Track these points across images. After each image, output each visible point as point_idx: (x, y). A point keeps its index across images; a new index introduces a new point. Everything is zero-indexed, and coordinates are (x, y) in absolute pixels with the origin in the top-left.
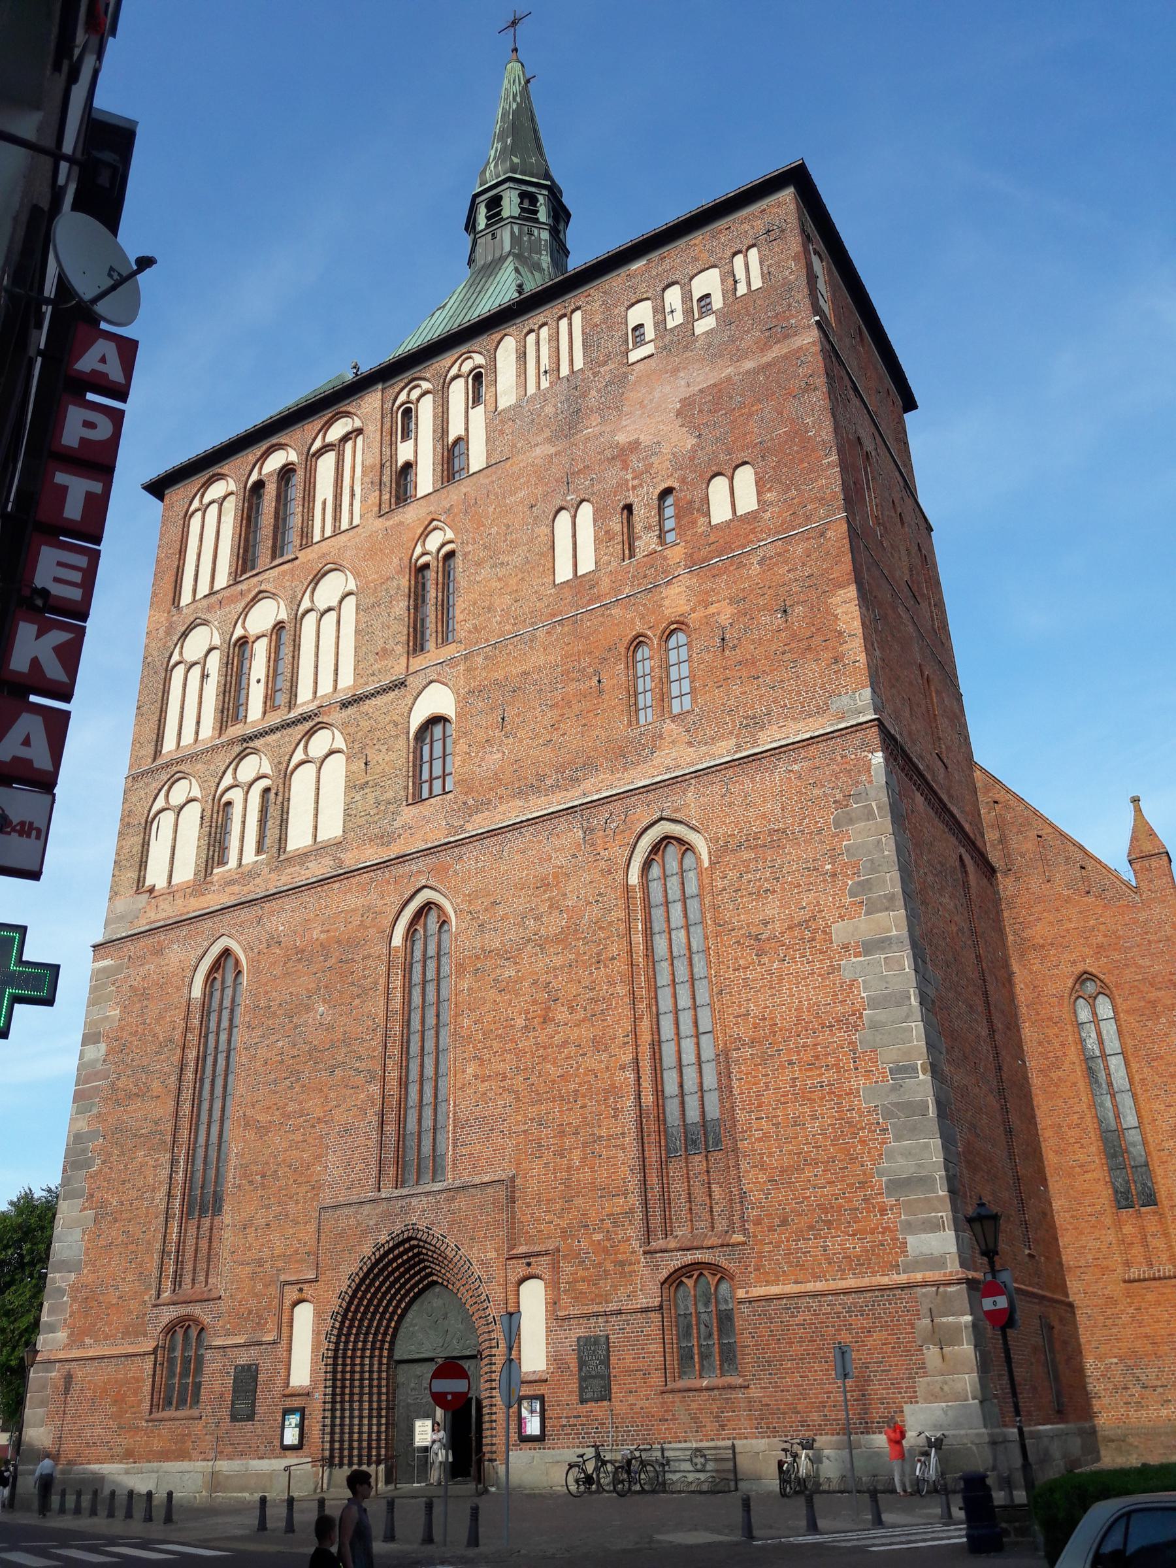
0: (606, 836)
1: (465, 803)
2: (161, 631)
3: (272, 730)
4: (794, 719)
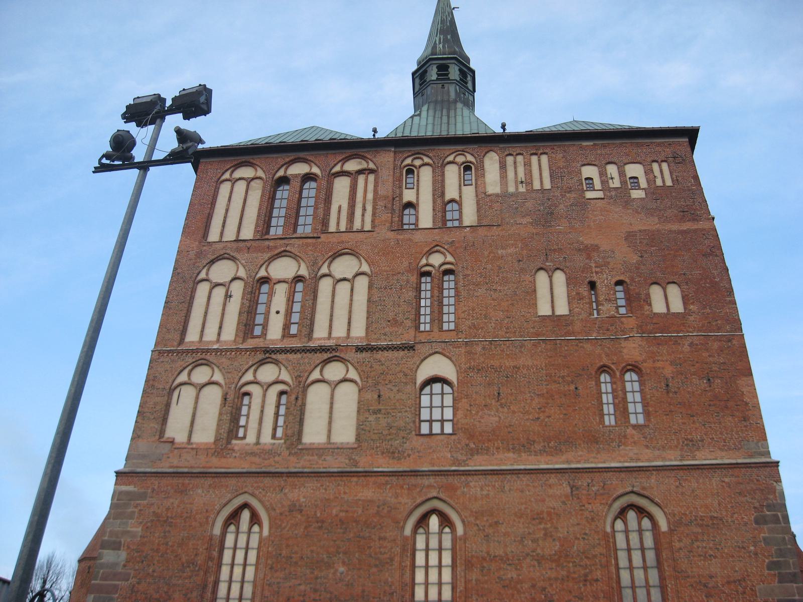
0: (589, 495)
1: (467, 445)
2: (192, 254)
4: (720, 449)
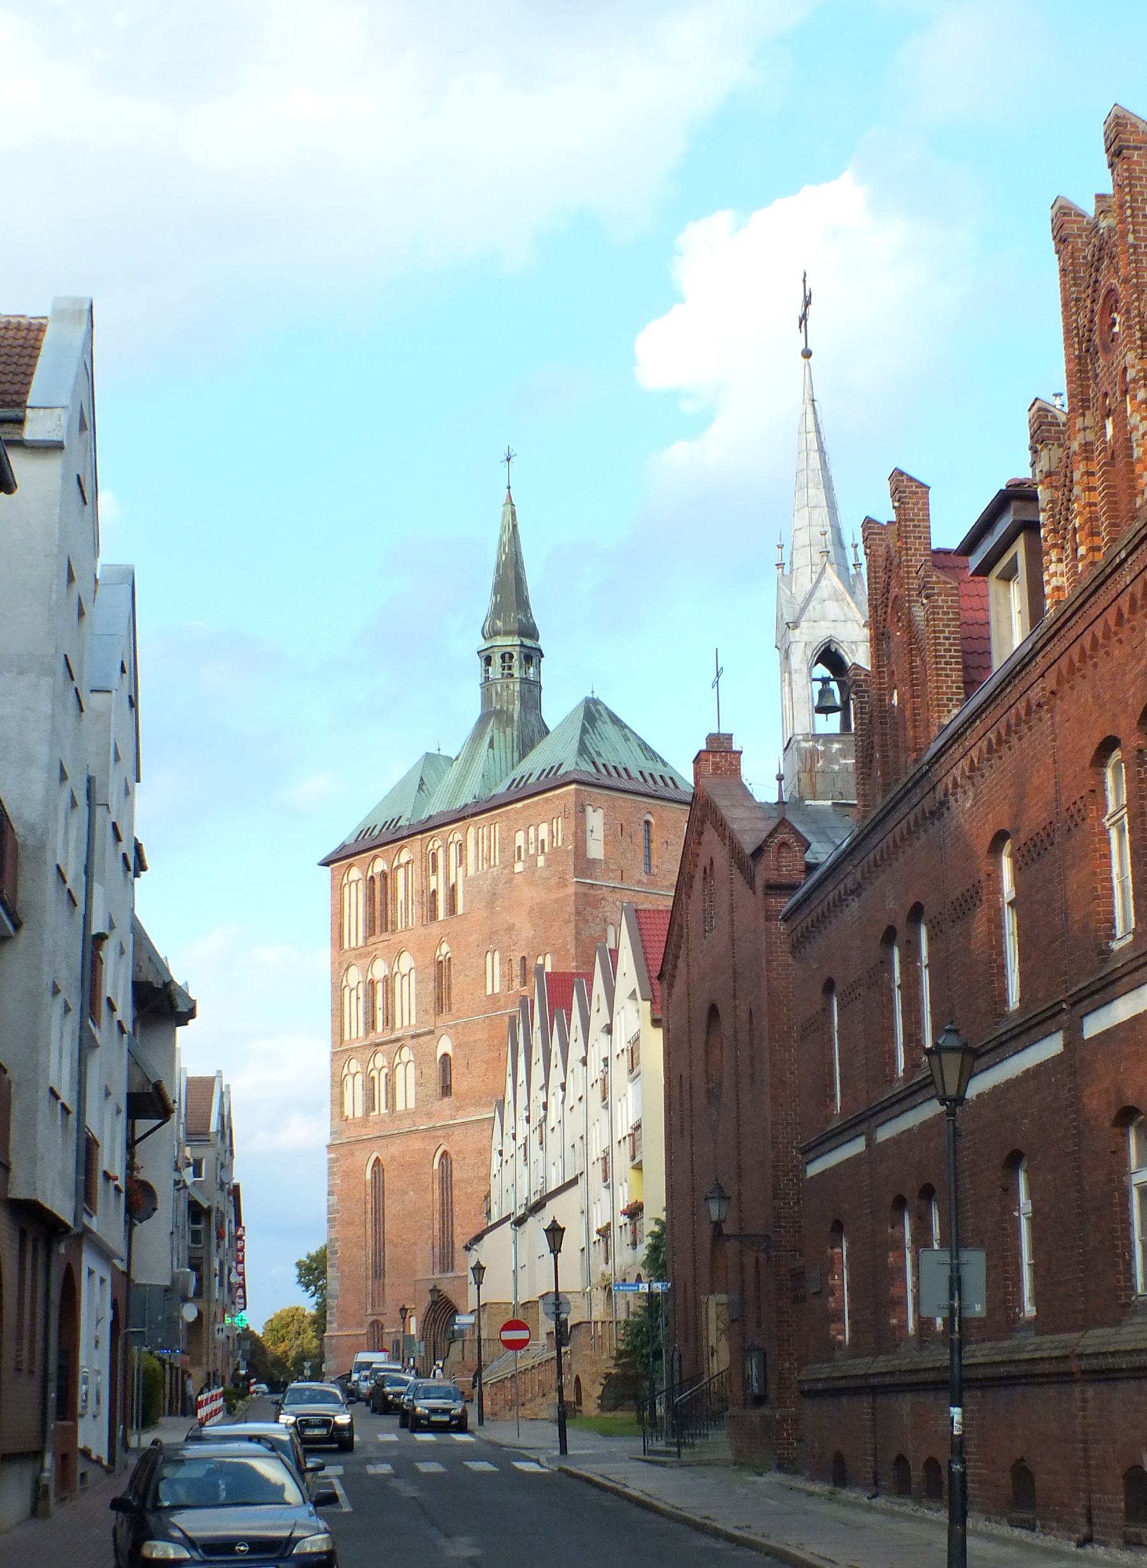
3: (387, 1043)
